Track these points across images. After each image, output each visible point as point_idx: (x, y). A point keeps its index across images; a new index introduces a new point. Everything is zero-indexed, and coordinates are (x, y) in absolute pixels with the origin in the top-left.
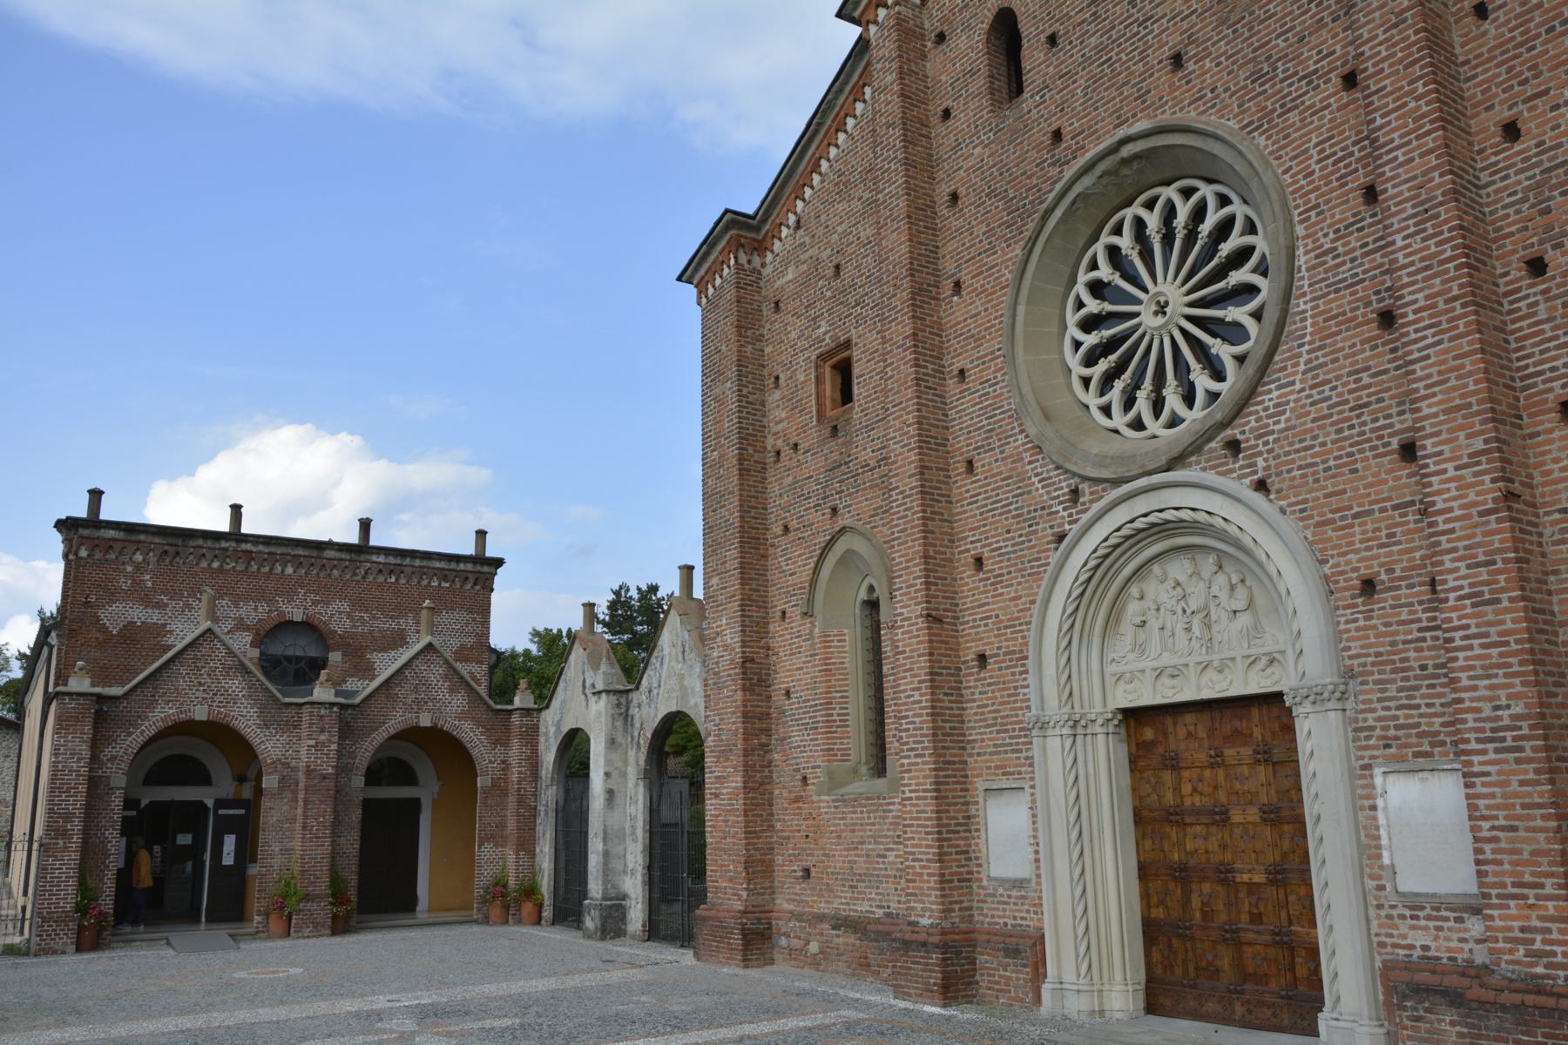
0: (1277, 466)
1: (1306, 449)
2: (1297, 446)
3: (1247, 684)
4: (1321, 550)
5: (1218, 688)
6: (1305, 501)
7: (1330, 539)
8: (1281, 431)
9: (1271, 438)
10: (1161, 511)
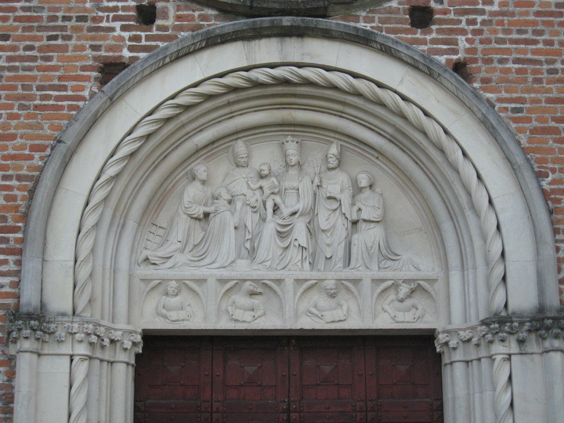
0: (484, 51)
1: (527, 42)
2: (515, 36)
3: (375, 317)
4: (538, 161)
5: (329, 316)
7: (551, 151)
8: (493, 14)
9: (479, 18)
10: (300, 66)
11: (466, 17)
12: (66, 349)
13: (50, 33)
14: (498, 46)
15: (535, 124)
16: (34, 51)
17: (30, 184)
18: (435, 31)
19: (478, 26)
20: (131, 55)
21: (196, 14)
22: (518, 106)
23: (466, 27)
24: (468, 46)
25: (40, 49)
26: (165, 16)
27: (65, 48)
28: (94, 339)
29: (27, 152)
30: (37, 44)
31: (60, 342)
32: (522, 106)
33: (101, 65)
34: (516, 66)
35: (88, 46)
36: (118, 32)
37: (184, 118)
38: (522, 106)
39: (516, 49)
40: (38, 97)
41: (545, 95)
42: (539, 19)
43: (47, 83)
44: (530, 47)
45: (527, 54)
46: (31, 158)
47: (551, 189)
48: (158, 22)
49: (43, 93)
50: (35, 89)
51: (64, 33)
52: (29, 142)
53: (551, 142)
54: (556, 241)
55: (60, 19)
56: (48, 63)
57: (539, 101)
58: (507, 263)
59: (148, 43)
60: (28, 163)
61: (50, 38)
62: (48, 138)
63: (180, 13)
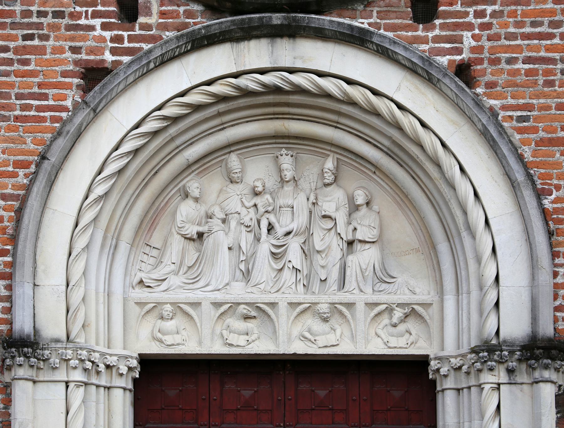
0: (492, 50)
2: (528, 30)
6: (528, 107)
11: (474, 8)
12: (61, 375)
13: (26, 32)
14: (507, 43)
15: (542, 134)
16: (9, 53)
17: (16, 204)
18: (438, 27)
19: (486, 20)
20: (114, 58)
21: (182, 9)
22: (524, 113)
23: (473, 21)
24: (474, 43)
25: (16, 51)
26: (149, 14)
27: (41, 50)
28: (89, 365)
29: (10, 169)
30: (12, 45)
31: (54, 369)
32: (529, 113)
33: (83, 70)
34: (527, 66)
35: (67, 48)
36: (98, 32)
37: (173, 131)
38: (529, 113)
39: (528, 45)
40: (18, 107)
41: (556, 100)
42: (559, 6)
43: (27, 91)
44: (544, 42)
45: (539, 52)
46: (15, 175)
47: (554, 209)
48: (142, 20)
49: (23, 102)
50: (13, 97)
51: (41, 32)
52: (12, 158)
53: (558, 155)
54: (556, 265)
55: (35, 15)
56: (26, 68)
57: (549, 108)
58: (500, 288)
59: (131, 45)
60: (13, 180)
61: (26, 38)
62: (31, 153)
63: (163, 8)
